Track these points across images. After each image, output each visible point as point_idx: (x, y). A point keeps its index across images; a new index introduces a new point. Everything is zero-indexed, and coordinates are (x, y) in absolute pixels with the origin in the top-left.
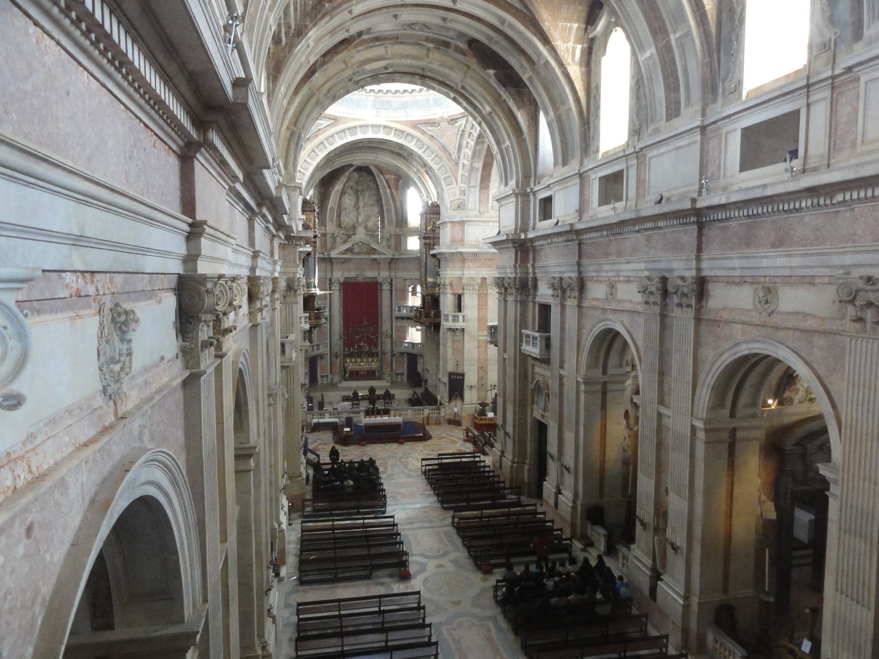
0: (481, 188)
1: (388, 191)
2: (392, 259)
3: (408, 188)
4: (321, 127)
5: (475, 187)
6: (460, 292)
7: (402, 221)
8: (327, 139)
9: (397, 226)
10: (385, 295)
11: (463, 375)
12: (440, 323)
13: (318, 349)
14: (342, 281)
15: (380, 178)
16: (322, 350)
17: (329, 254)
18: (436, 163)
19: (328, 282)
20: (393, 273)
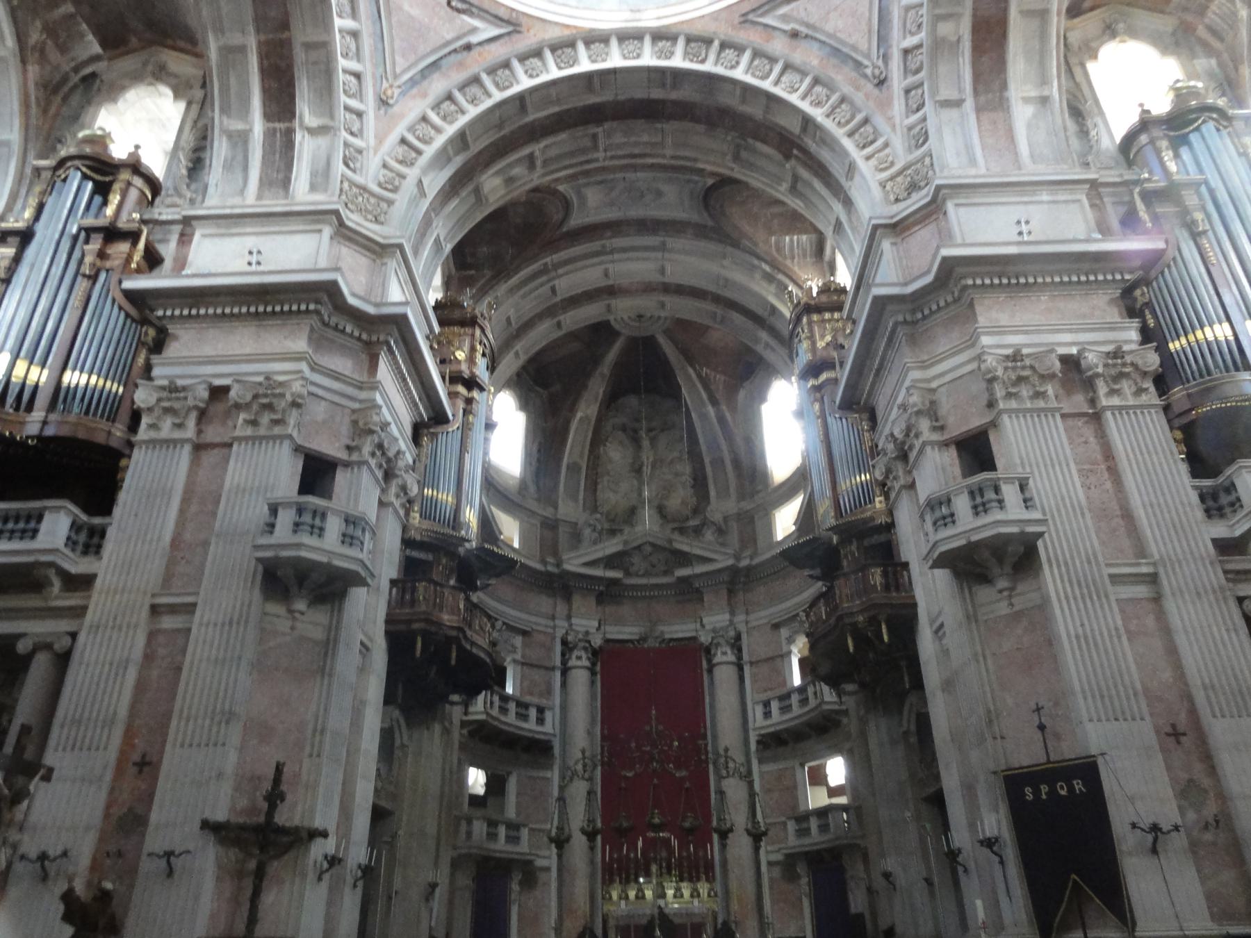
0: (979, 110)
1: (711, 410)
2: (734, 572)
3: (762, 398)
4: (474, 39)
5: (958, 103)
6: (975, 422)
7: (750, 472)
8: (491, 71)
9: (742, 497)
10: (724, 676)
11: (1088, 770)
12: (915, 605)
13: (513, 839)
14: (597, 641)
15: (689, 378)
16: (524, 847)
17: (558, 565)
18: (818, 104)
19: (558, 648)
20: (740, 618)
